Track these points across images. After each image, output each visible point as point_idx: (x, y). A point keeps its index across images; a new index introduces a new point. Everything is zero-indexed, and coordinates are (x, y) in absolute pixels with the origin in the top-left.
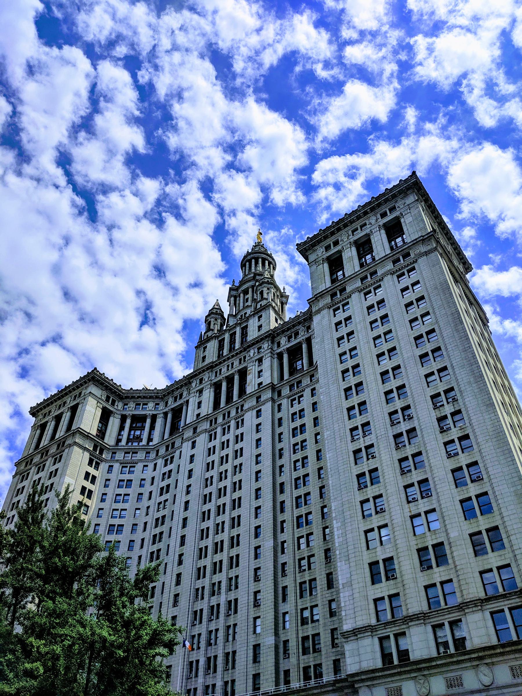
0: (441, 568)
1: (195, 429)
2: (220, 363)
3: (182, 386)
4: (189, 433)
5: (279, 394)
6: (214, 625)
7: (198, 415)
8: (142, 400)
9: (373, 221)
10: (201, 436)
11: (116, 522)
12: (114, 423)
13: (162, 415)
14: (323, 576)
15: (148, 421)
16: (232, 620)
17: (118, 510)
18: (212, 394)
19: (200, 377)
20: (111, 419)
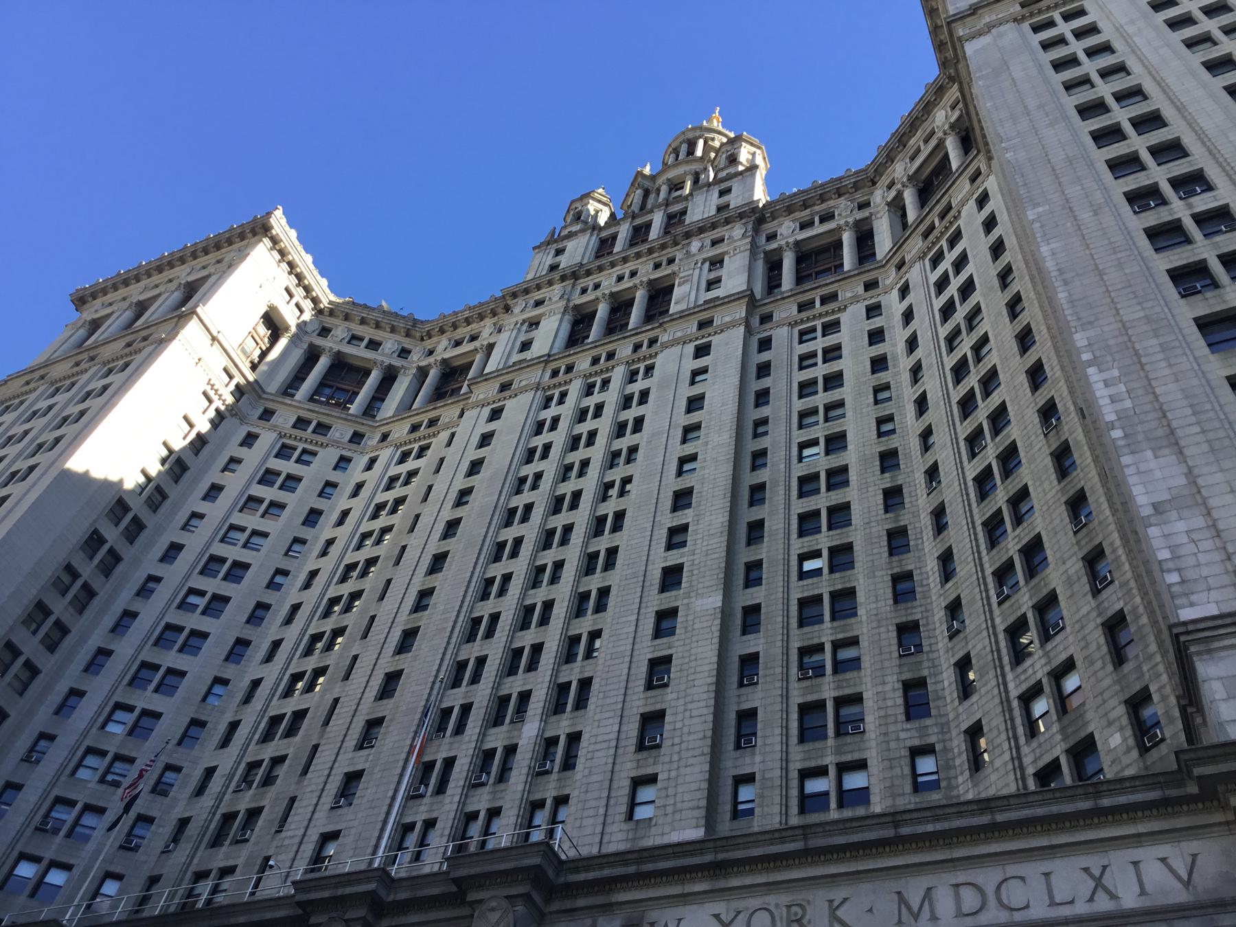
2: (601, 269)
3: (481, 317)
5: (766, 318)
6: (486, 797)
8: (372, 331)
11: (233, 553)
14: (888, 687)
16: (552, 785)
17: (243, 529)
19: (537, 296)
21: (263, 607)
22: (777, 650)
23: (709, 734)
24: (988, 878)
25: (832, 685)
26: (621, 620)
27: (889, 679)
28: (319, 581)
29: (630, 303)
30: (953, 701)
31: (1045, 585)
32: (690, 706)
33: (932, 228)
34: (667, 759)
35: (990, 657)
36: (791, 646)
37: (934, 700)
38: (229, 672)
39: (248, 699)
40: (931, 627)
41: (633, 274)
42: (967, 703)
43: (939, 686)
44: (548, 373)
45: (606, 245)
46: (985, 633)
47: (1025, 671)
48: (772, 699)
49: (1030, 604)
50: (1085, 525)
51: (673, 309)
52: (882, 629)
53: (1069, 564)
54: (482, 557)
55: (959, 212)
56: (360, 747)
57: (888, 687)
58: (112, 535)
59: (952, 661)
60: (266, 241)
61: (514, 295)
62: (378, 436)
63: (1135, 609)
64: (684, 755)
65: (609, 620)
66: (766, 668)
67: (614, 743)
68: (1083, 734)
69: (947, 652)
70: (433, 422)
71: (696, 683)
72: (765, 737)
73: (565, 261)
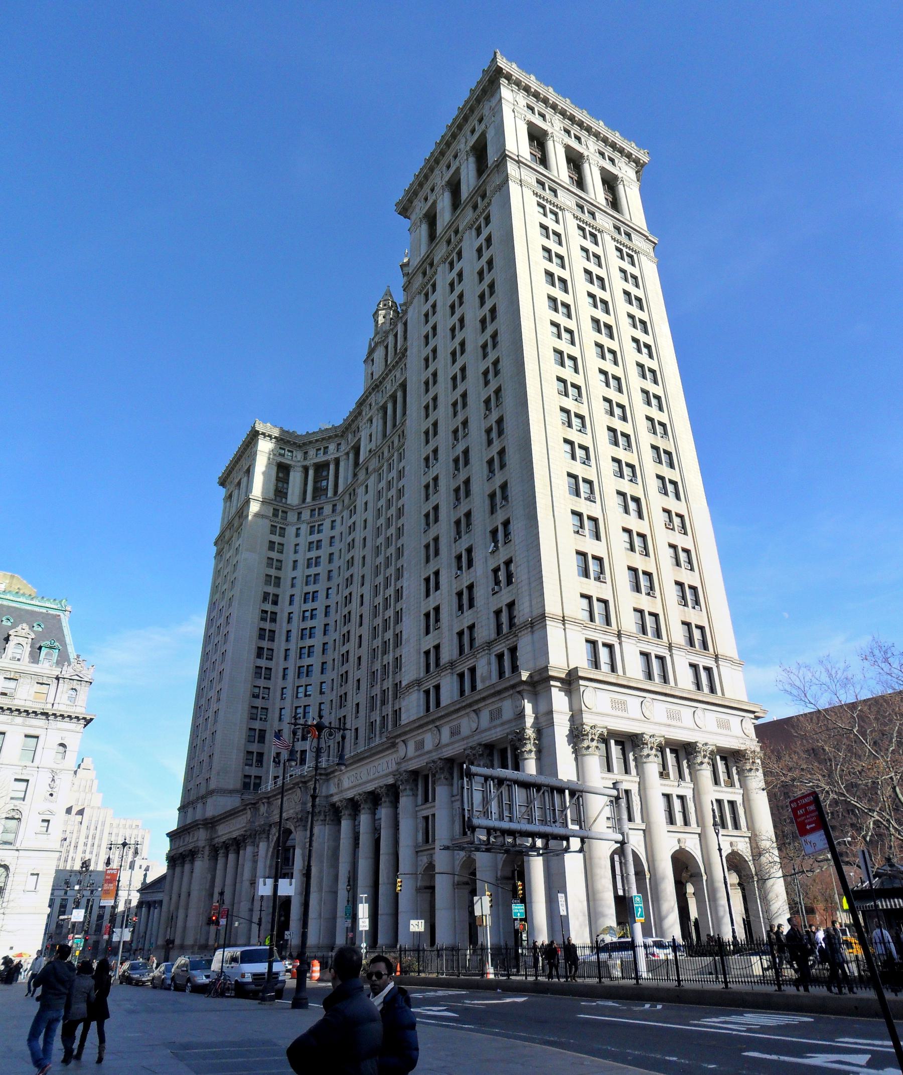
0: (470, 612)
1: (367, 469)
2: (384, 379)
3: (356, 417)
4: (362, 476)
7: (370, 451)
9: (462, 146)
12: (296, 478)
15: (332, 467)
18: (381, 422)
19: (368, 402)
20: (292, 474)
21: (327, 607)
24: (376, 764)
56: (359, 669)
58: (268, 607)
60: (261, 437)
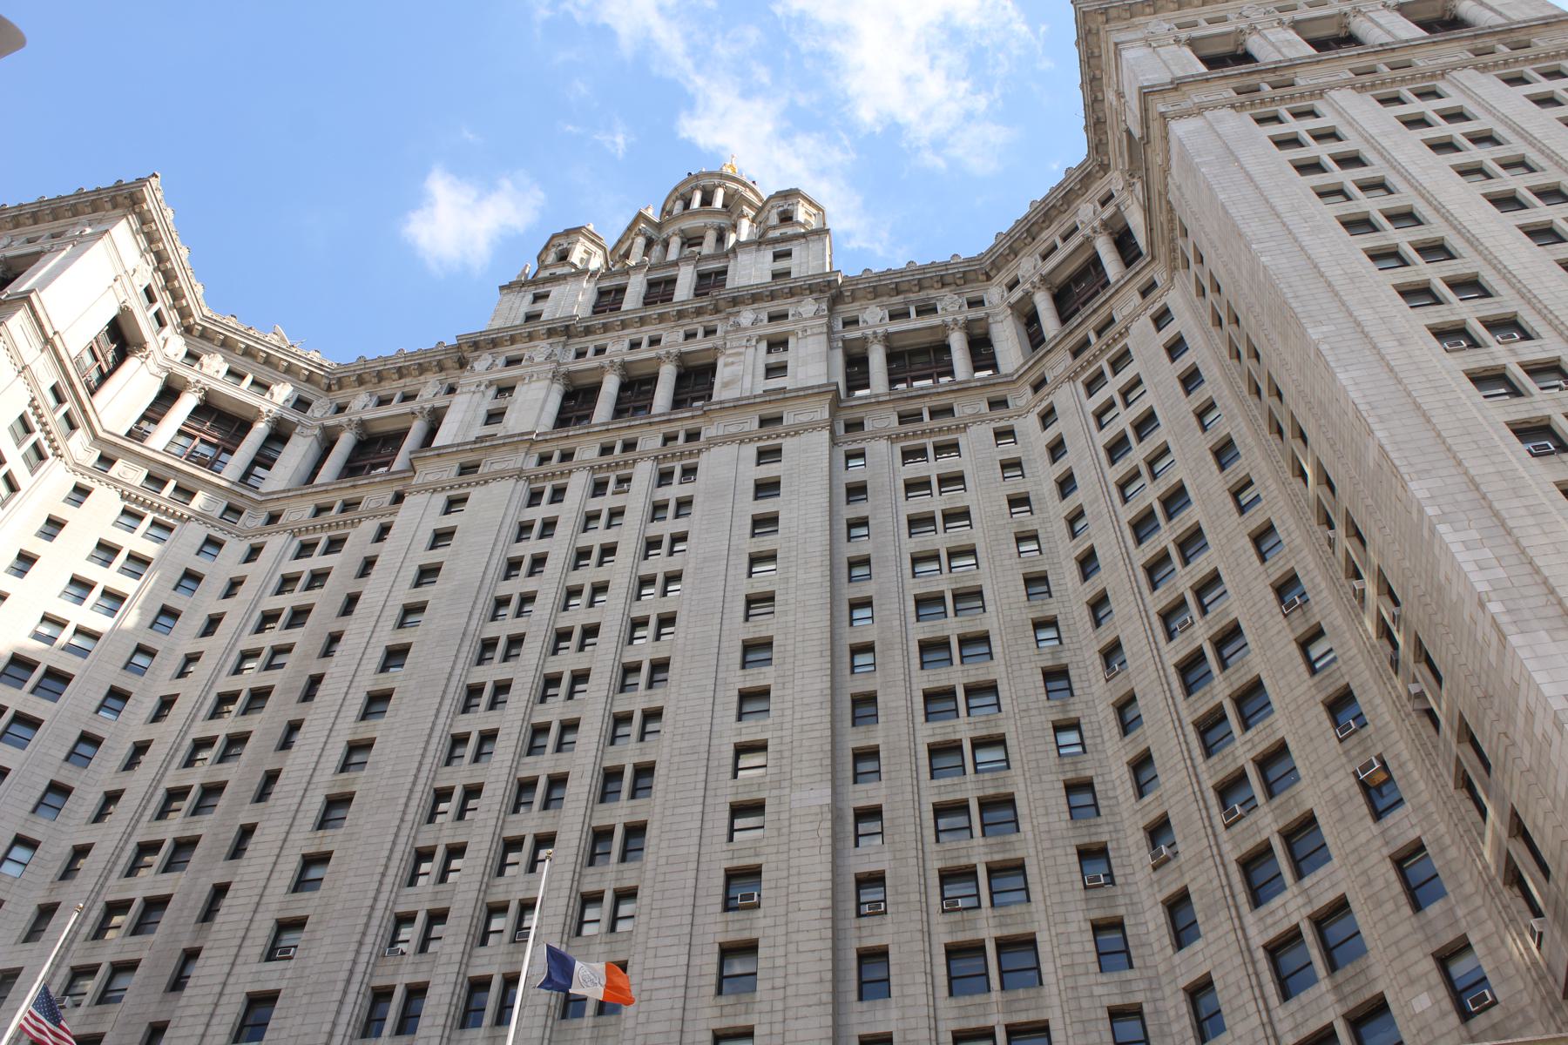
3: (422, 369)
10: (492, 485)
13: (317, 431)
14: (1073, 927)
19: (512, 351)
22: (911, 869)
23: (829, 976)
25: (991, 921)
26: (678, 811)
27: (1071, 916)
28: (178, 712)
29: (652, 380)
30: (1162, 949)
31: (1297, 805)
32: (794, 937)
33: (1086, 343)
34: (766, 1007)
35: (1219, 894)
36: (929, 865)
37: (1136, 947)
38: (37, 829)
39: (68, 872)
40: (1124, 852)
41: (655, 342)
42: (1185, 952)
43: (1143, 930)
44: (535, 459)
45: (608, 299)
46: (1210, 862)
47: (1272, 912)
48: (913, 933)
49: (1275, 828)
50: (1355, 731)
51: (719, 393)
52: (1058, 852)
53: (1332, 780)
54: (447, 702)
55: (1127, 329)
56: (270, 956)
57: (1073, 927)
59: (1161, 897)
61: (476, 346)
62: (264, 517)
63: (1438, 840)
64: (791, 1002)
65: (657, 810)
66: (897, 893)
67: (682, 981)
68: (1368, 994)
69: (1151, 885)
70: (348, 506)
71: (802, 905)
72: (902, 985)
73: (548, 310)
